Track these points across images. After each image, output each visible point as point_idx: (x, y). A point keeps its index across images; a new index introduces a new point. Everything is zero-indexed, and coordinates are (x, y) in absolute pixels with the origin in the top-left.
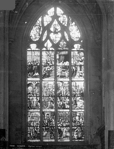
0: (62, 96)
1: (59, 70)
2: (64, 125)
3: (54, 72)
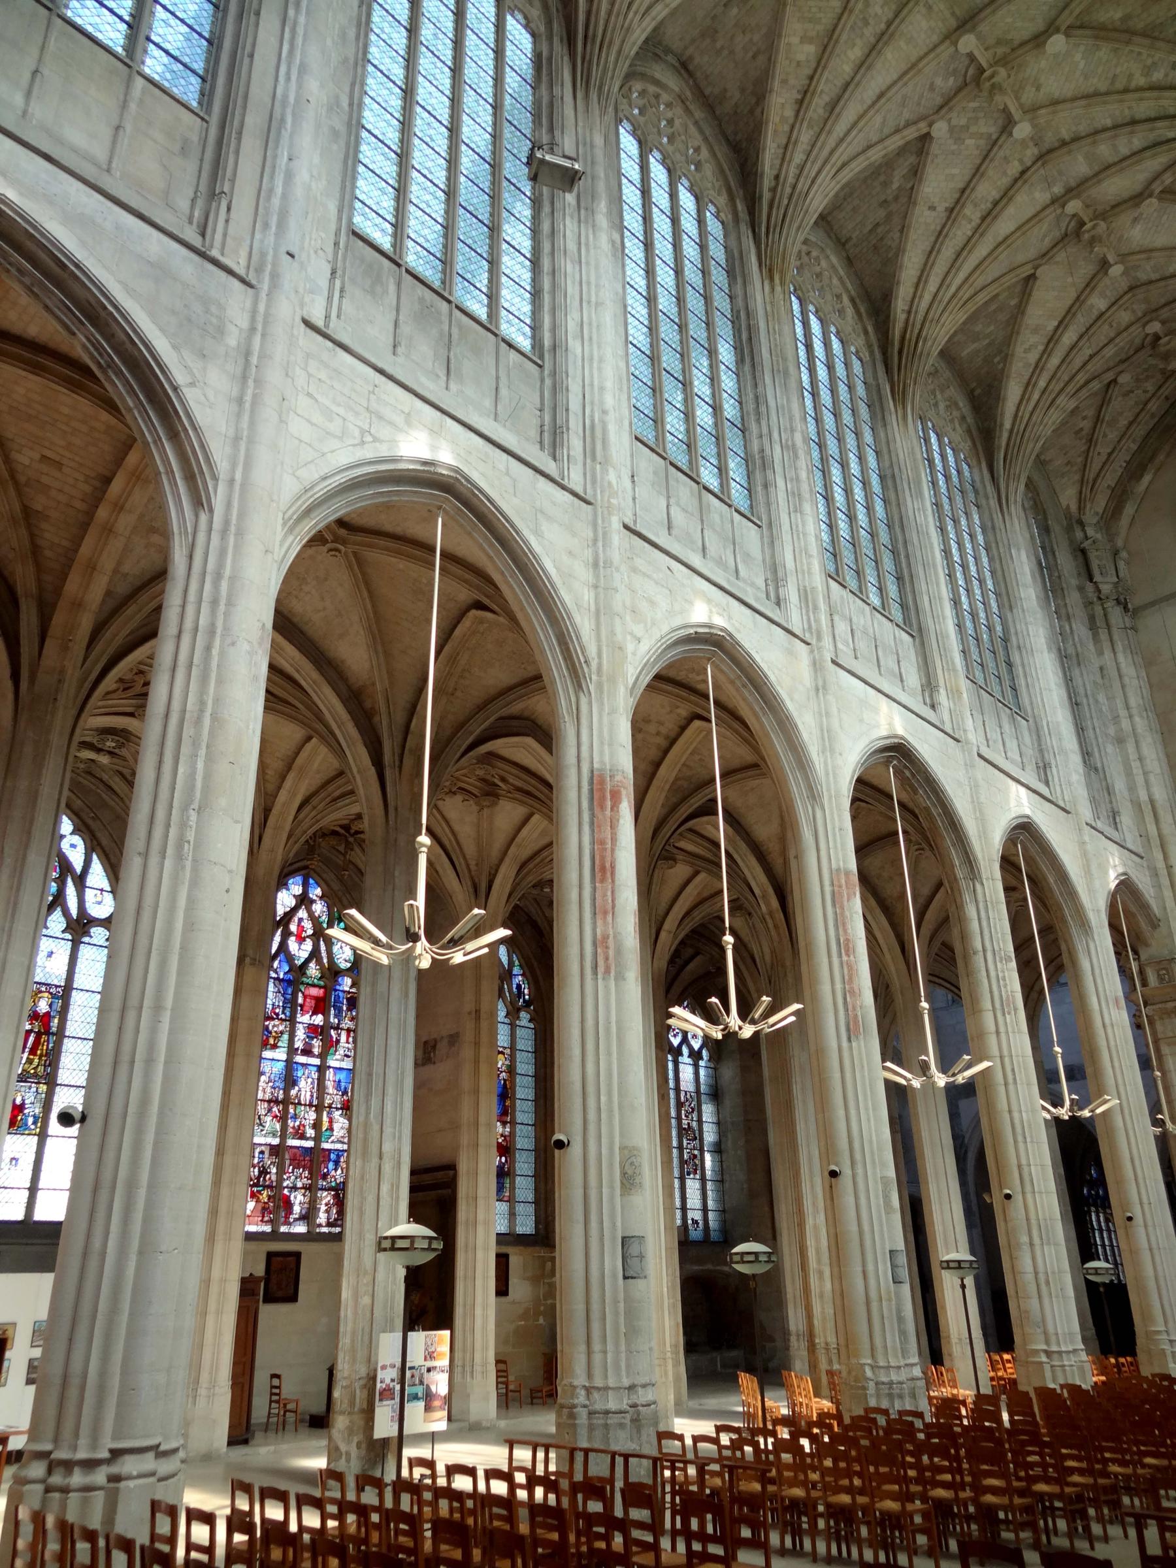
0: (299, 1104)
1: (301, 1034)
2: (299, 1185)
3: (286, 1037)
